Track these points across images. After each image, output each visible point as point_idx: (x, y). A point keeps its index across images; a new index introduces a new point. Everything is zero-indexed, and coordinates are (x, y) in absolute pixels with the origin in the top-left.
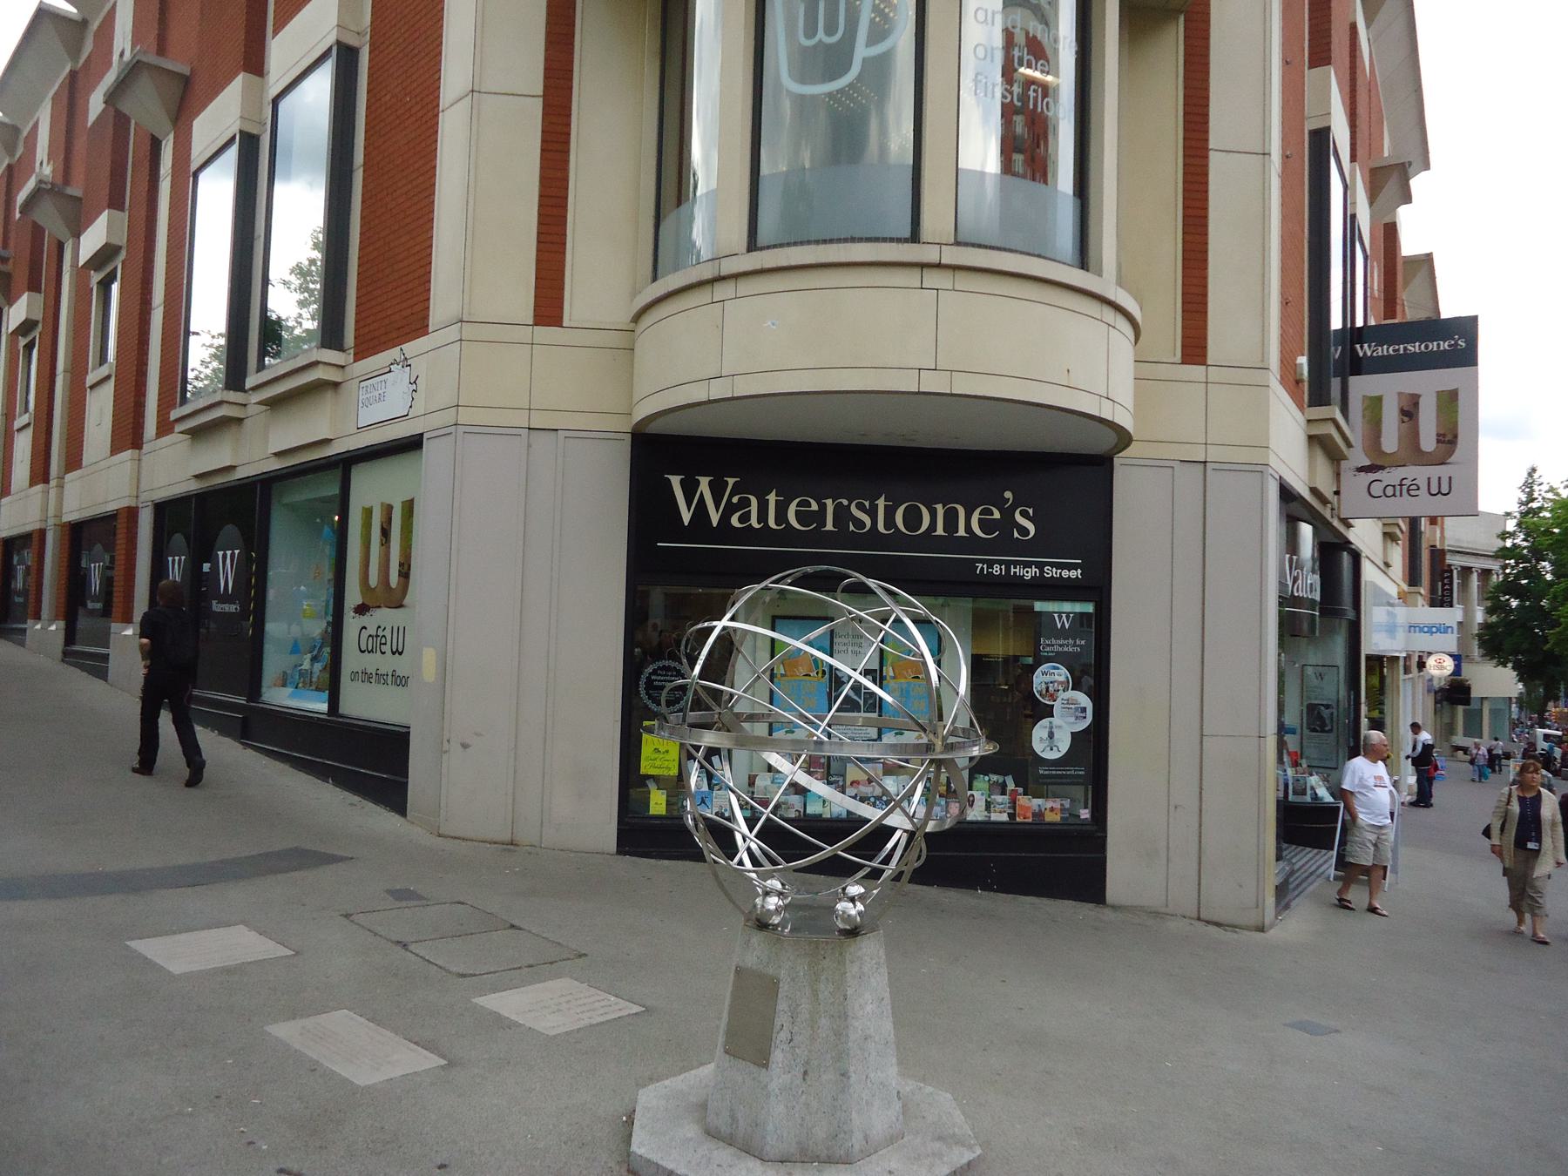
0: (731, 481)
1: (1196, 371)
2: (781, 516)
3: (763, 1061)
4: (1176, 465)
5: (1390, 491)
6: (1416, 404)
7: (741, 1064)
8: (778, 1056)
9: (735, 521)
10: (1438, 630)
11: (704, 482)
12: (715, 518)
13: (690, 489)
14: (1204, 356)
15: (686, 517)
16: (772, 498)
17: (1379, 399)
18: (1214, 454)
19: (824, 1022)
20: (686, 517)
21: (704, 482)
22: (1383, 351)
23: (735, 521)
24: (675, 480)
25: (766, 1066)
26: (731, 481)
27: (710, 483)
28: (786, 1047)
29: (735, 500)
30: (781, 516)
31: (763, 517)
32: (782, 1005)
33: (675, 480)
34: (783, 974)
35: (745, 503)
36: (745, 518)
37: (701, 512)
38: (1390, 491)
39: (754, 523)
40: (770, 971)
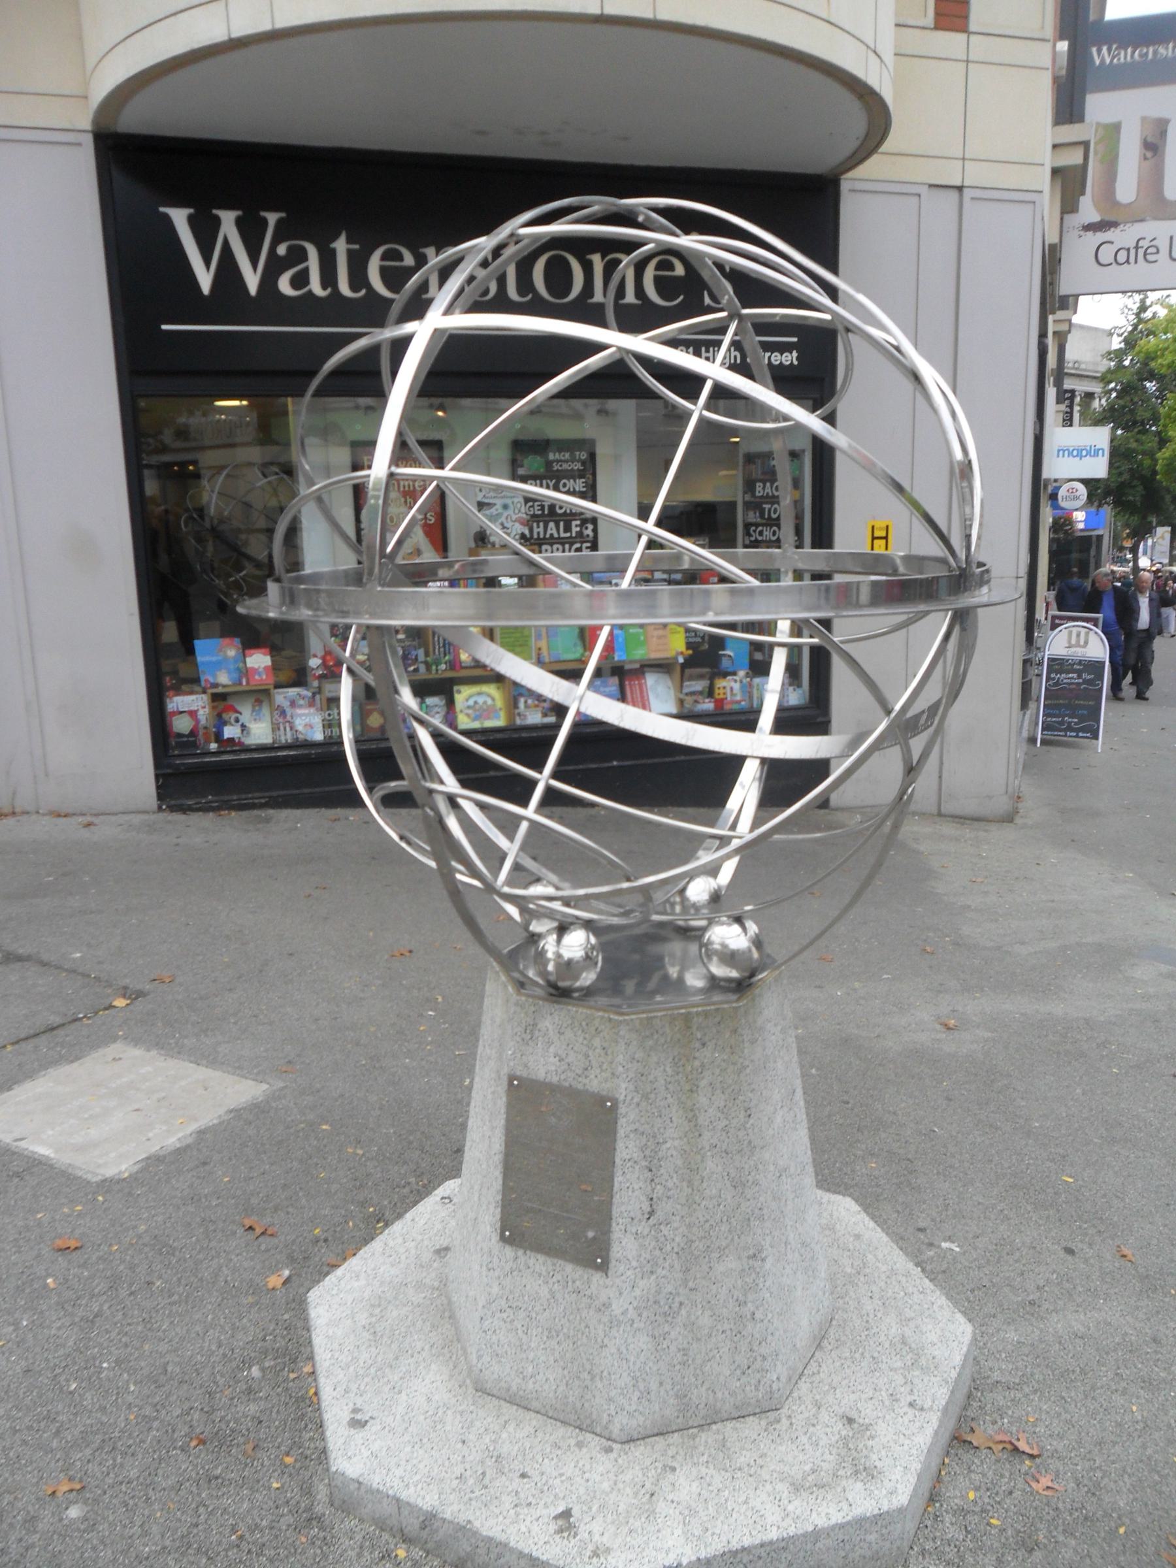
0: (272, 218)
1: (952, 42)
2: (358, 278)
3: (594, 1255)
4: (924, 190)
5: (1122, 257)
6: (1163, 134)
7: (538, 1263)
8: (625, 1245)
9: (284, 285)
10: (1089, 453)
11: (228, 220)
12: (252, 281)
13: (206, 232)
14: (966, 17)
15: (205, 280)
16: (341, 246)
17: (1116, 128)
18: (975, 175)
19: (712, 1165)
20: (205, 280)
21: (228, 220)
22: (1126, 56)
23: (284, 285)
24: (179, 217)
25: (604, 1268)
26: (272, 218)
27: (239, 223)
28: (644, 1228)
29: (282, 250)
30: (358, 278)
31: (328, 278)
32: (626, 1149)
33: (179, 217)
34: (623, 1090)
35: (298, 255)
36: (300, 280)
37: (228, 272)
38: (1122, 257)
39: (315, 286)
40: (595, 1083)
